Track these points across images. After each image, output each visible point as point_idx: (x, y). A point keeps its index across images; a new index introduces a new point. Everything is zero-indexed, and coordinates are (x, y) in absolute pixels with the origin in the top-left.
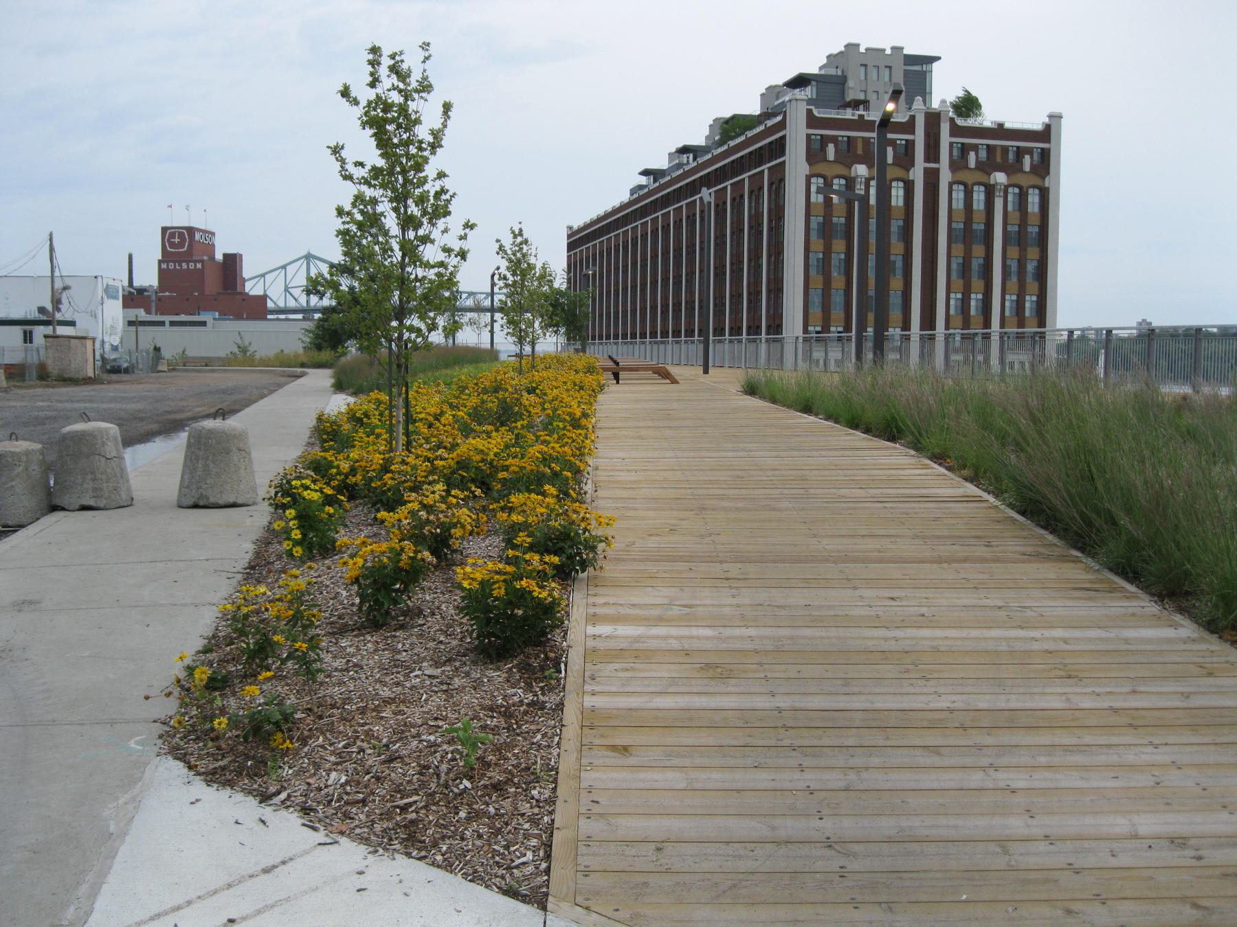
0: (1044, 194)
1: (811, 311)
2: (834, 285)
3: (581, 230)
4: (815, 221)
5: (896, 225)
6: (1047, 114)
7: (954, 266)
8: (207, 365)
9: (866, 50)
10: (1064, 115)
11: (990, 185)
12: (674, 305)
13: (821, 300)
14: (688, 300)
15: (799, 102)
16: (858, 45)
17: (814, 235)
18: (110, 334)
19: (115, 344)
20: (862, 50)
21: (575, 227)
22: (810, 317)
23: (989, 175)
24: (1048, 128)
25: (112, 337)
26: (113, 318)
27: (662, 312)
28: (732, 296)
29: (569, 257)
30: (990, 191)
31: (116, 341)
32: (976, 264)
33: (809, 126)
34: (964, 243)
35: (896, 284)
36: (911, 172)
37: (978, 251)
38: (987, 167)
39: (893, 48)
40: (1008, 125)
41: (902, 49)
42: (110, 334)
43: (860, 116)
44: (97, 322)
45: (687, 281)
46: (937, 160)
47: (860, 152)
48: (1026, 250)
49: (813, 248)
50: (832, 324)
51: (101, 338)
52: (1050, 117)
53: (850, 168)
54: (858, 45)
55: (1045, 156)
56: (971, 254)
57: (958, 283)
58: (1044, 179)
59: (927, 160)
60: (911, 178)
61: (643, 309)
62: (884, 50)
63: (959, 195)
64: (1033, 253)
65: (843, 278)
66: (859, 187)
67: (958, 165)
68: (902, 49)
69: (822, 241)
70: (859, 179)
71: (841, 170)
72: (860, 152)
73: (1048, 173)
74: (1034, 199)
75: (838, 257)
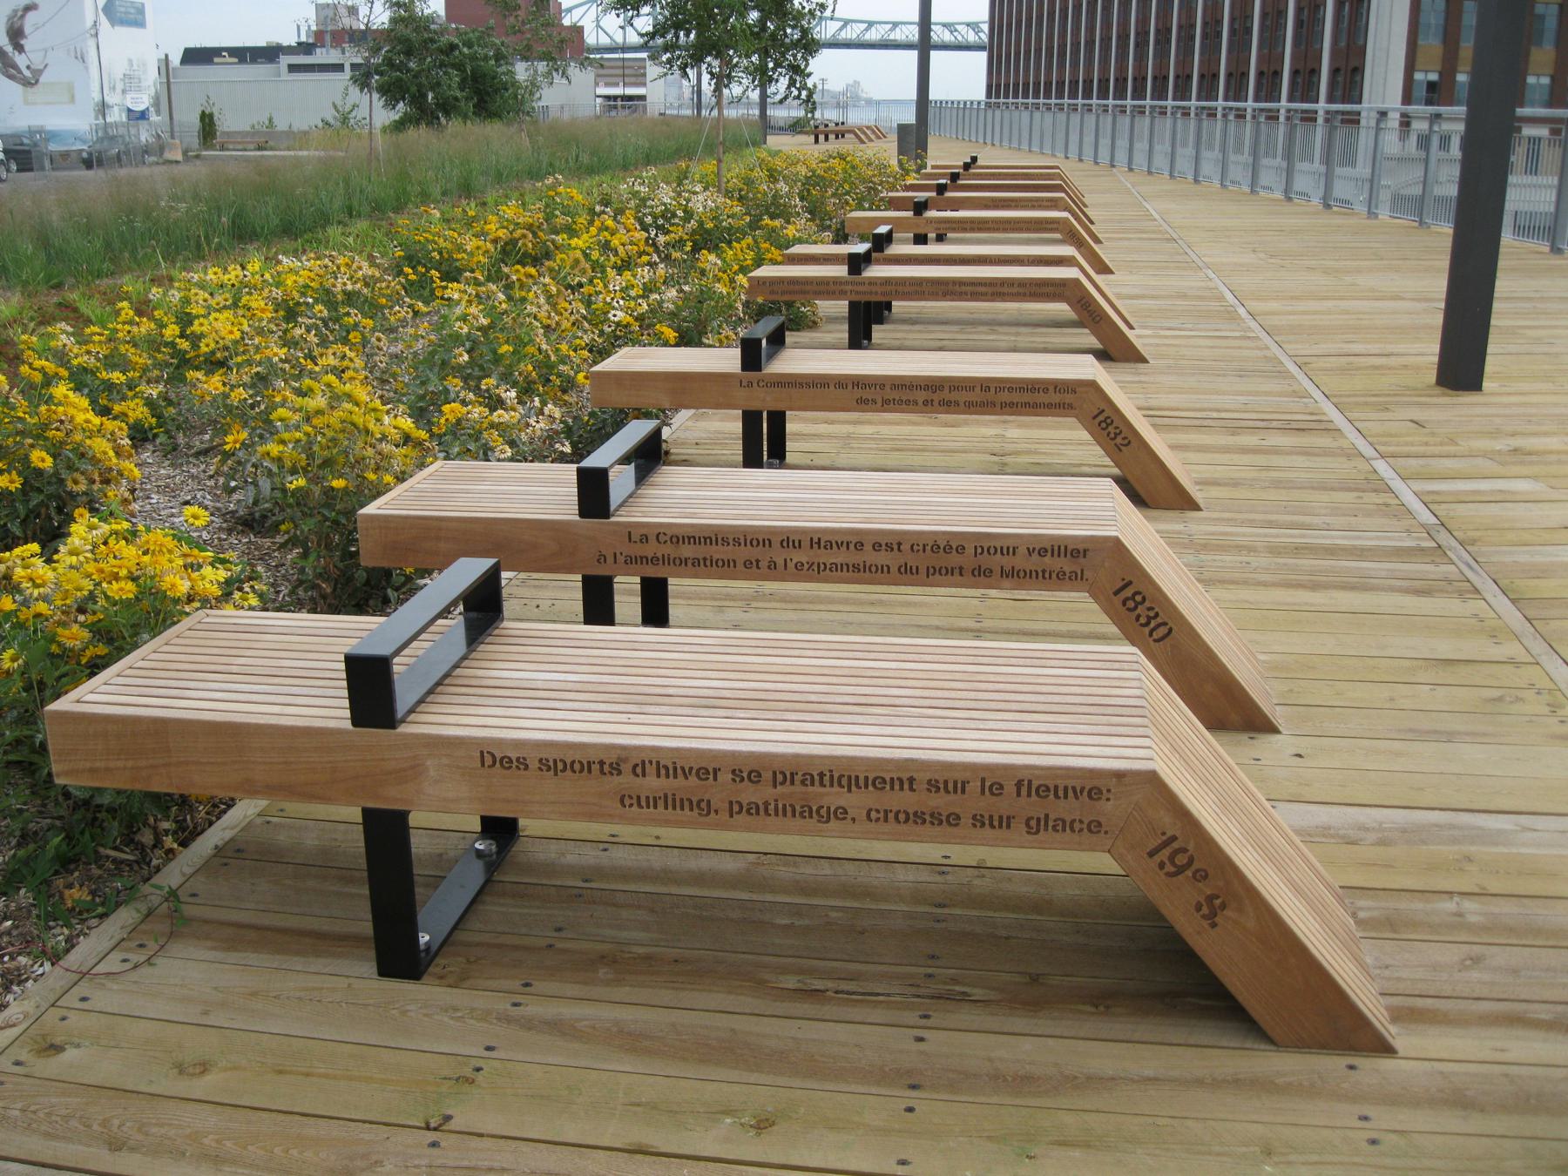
1: (1420, 42)
8: (260, 148)
12: (1158, 31)
13: (1442, 22)
14: (1183, 22)
18: (124, 92)
19: (141, 108)
25: (128, 97)
26: (130, 61)
27: (1137, 45)
28: (1264, 15)
31: (142, 102)
42: (124, 92)
44: (87, 68)
50: (1460, 69)
51: (97, 97)
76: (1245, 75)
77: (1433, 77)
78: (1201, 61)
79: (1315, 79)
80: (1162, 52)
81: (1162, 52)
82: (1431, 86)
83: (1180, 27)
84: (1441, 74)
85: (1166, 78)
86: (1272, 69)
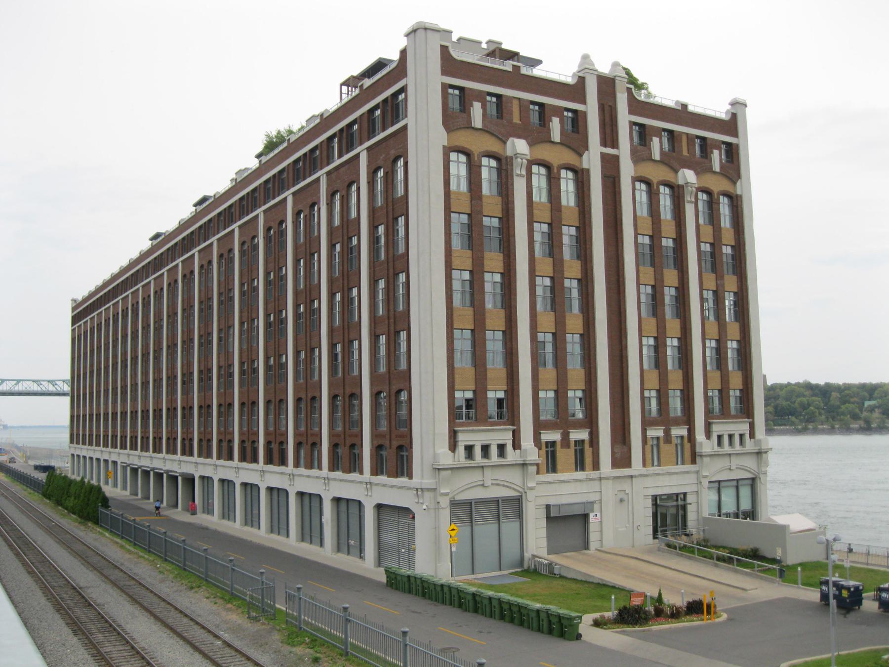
0: (736, 204)
2: (489, 323)
3: (85, 300)
4: (459, 220)
5: (568, 233)
6: (729, 101)
7: (643, 298)
9: (460, 39)
10: (748, 105)
11: (679, 186)
14: (222, 363)
15: (428, 31)
16: (451, 32)
17: (456, 242)
20: (455, 38)
21: (80, 298)
22: (457, 376)
23: (676, 172)
24: (734, 116)
27: (183, 382)
29: (73, 331)
30: (677, 193)
32: (669, 293)
33: (445, 72)
34: (653, 264)
35: (574, 322)
36: (585, 156)
37: (671, 277)
38: (672, 160)
39: (489, 42)
40: (691, 108)
41: (501, 44)
43: (514, 66)
45: (220, 339)
46: (615, 144)
47: (516, 120)
48: (722, 278)
49: (456, 263)
50: (489, 387)
52: (734, 104)
53: (505, 143)
54: (451, 32)
55: (732, 153)
56: (663, 281)
57: (651, 325)
58: (734, 183)
59: (604, 143)
60: (585, 166)
61: (158, 381)
62: (480, 43)
63: (642, 196)
64: (731, 282)
65: (502, 313)
66: (519, 172)
67: (640, 154)
68: (501, 44)
69: (469, 253)
70: (519, 160)
71: (492, 145)
72: (516, 120)
73: (739, 176)
74: (725, 209)
75: (492, 280)
76: (283, 401)
77: (469, 395)
78: (240, 393)
79: (317, 405)
80: (205, 385)
81: (205, 385)
82: (469, 403)
83: (220, 367)
84: (474, 392)
85: (210, 407)
86: (310, 396)
